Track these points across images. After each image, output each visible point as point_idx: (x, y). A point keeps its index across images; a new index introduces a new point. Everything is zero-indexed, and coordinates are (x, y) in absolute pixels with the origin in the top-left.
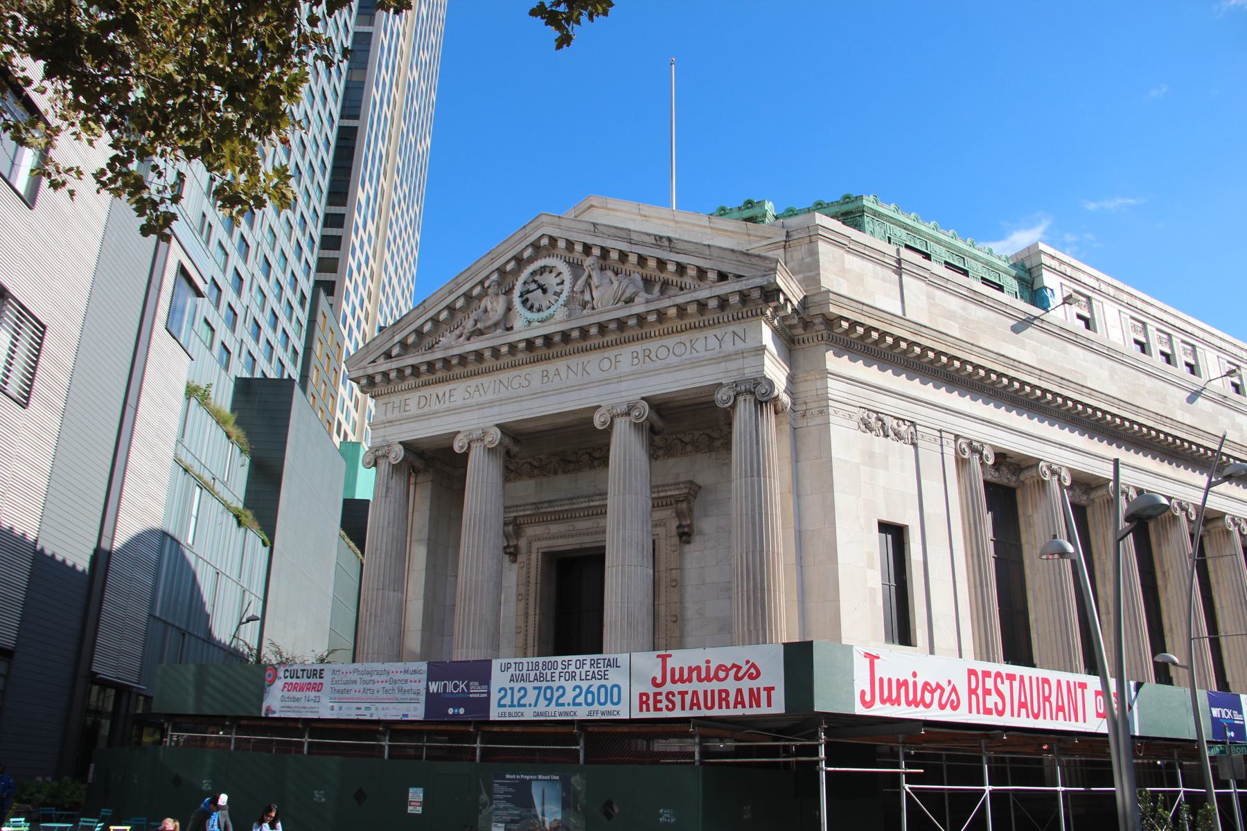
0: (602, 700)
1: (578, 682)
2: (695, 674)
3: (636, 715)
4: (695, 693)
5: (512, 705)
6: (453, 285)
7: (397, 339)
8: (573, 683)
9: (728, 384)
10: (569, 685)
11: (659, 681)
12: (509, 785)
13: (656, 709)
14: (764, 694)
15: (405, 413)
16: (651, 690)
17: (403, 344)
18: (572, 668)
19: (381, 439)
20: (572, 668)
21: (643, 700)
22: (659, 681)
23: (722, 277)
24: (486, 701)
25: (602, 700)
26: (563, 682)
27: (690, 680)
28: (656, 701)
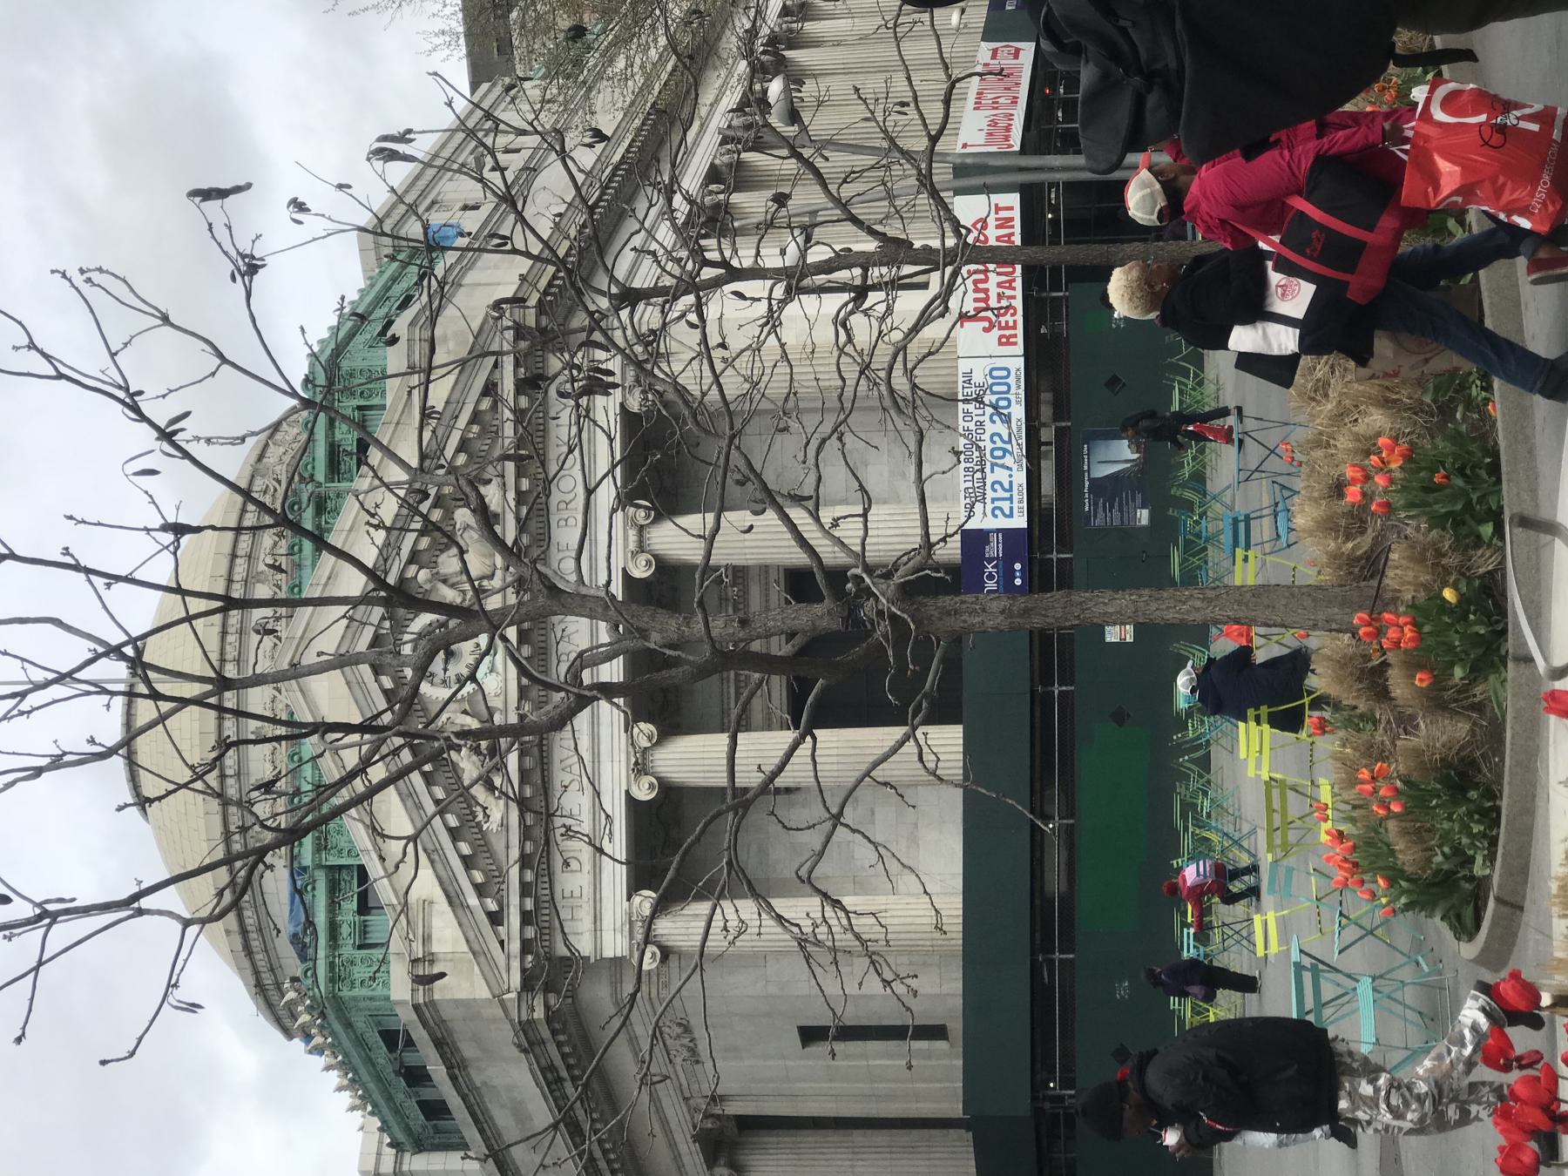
0: (1005, 388)
1: (987, 418)
2: (981, 286)
3: (1019, 349)
4: (999, 285)
5: (1011, 499)
6: (409, 802)
7: (473, 900)
8: (988, 423)
9: (624, 396)
10: (990, 428)
11: (986, 324)
12: (1096, 504)
13: (1014, 327)
14: (1003, 214)
15: (585, 897)
16: (996, 333)
17: (480, 890)
18: (972, 426)
19: (619, 936)
20: (972, 426)
21: (1005, 341)
22: (986, 324)
23: (490, 389)
24: (1008, 534)
25: (1005, 388)
26: (986, 437)
27: (986, 291)
28: (1007, 327)
